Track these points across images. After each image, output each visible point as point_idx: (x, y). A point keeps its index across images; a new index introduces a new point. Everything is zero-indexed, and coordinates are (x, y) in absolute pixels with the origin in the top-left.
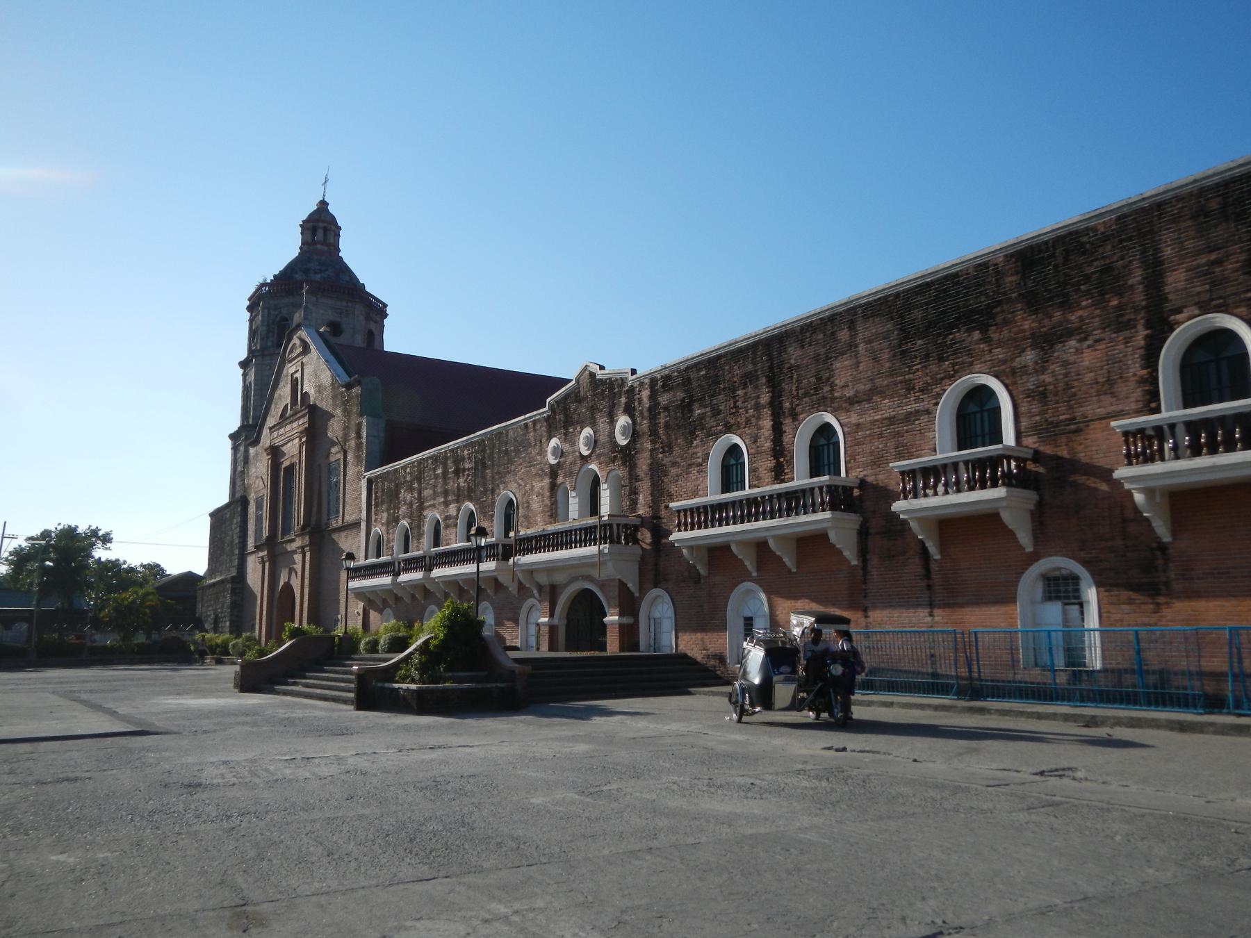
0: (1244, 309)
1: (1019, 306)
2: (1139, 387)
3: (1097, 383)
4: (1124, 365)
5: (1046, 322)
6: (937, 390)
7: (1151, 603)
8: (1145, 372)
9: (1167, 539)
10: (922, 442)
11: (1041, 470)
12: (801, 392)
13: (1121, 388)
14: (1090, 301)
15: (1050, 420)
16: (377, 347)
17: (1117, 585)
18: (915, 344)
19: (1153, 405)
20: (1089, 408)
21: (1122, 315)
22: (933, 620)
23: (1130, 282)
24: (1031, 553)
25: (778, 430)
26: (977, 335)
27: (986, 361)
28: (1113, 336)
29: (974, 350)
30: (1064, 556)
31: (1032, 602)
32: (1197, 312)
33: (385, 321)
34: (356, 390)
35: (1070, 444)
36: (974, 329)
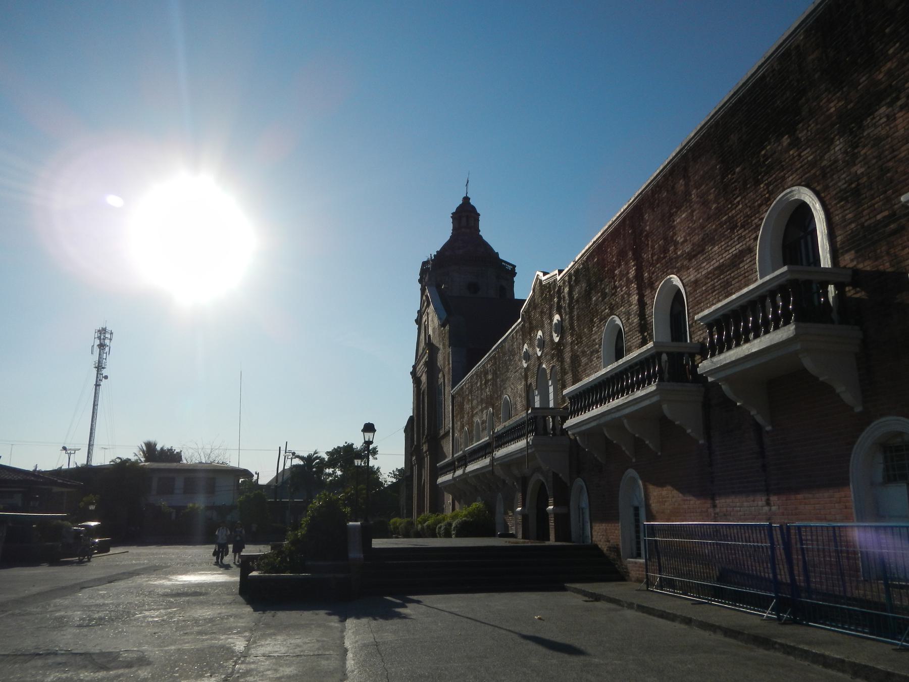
6: (756, 221)
11: (861, 295)
12: (655, 258)
14: (898, 45)
15: (866, 224)
18: (734, 173)
22: (770, 510)
25: (642, 304)
26: (786, 140)
33: (515, 279)
34: (447, 328)
35: (892, 251)
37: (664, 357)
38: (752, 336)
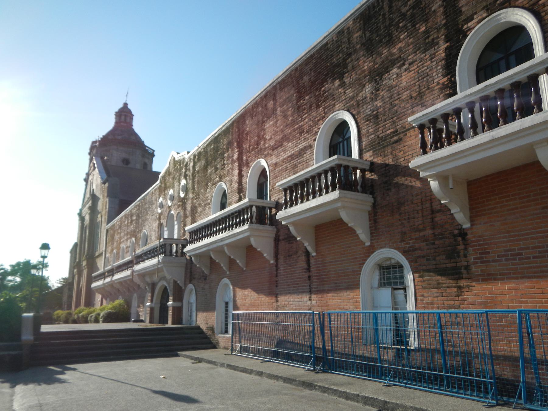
2: (441, 93)
4: (430, 77)
6: (316, 129)
7: (455, 287)
8: (446, 79)
9: (467, 225)
11: (375, 177)
12: (251, 147)
14: (406, 33)
15: (380, 136)
16: (149, 169)
17: (429, 271)
21: (428, 37)
22: (311, 303)
23: (433, 9)
25: (240, 175)
26: (337, 83)
30: (390, 247)
33: (154, 159)
34: (107, 185)
35: (394, 152)
36: (335, 79)
37: (254, 209)
38: (311, 197)
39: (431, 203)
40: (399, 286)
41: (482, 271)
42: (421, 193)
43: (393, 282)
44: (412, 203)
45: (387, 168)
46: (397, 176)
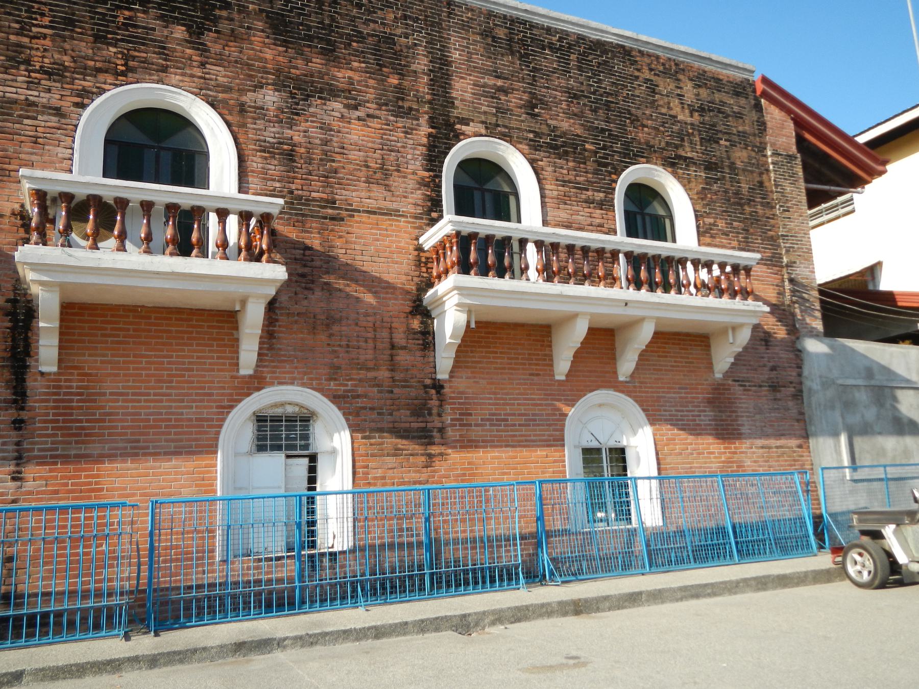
0: (527, 147)
1: (260, 25)
2: (419, 189)
3: (368, 167)
4: (402, 157)
5: (300, 63)
7: (422, 455)
8: (426, 174)
10: (34, 158)
13: (396, 182)
14: (363, 65)
17: (381, 430)
19: (434, 215)
20: (354, 194)
24: (250, 376)
27: (192, 76)
28: (392, 118)
29: (175, 50)
30: (303, 385)
31: (237, 454)
32: (483, 131)
39: (391, 333)
40: (298, 452)
41: (461, 436)
42: (375, 314)
43: (286, 445)
44: (357, 324)
45: (307, 253)
46: (327, 273)
